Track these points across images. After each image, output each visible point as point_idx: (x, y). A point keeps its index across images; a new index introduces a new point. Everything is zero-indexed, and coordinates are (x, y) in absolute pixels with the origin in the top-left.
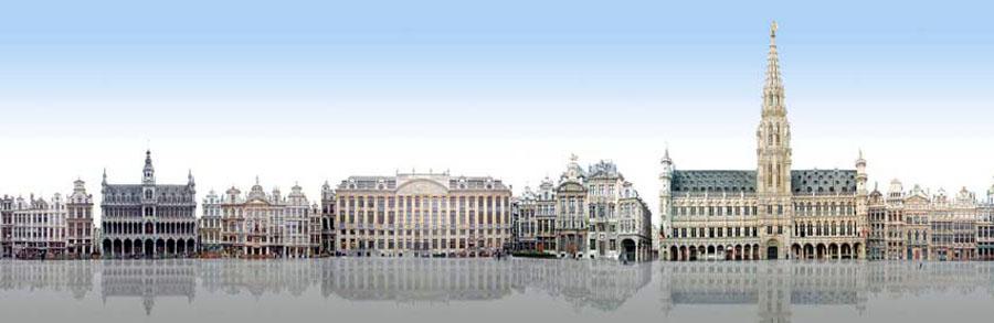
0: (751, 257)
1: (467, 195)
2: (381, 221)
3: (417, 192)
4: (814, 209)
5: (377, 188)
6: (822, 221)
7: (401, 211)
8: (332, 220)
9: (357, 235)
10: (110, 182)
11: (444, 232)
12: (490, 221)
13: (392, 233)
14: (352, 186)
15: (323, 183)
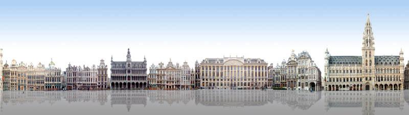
0: (359, 89)
1: (251, 66)
2: (218, 75)
3: (232, 65)
4: (383, 71)
5: (216, 63)
6: (387, 75)
8: (199, 75)
9: (209, 81)
10: (114, 60)
11: (242, 79)
12: (259, 76)
13: (222, 80)
15: (195, 61)
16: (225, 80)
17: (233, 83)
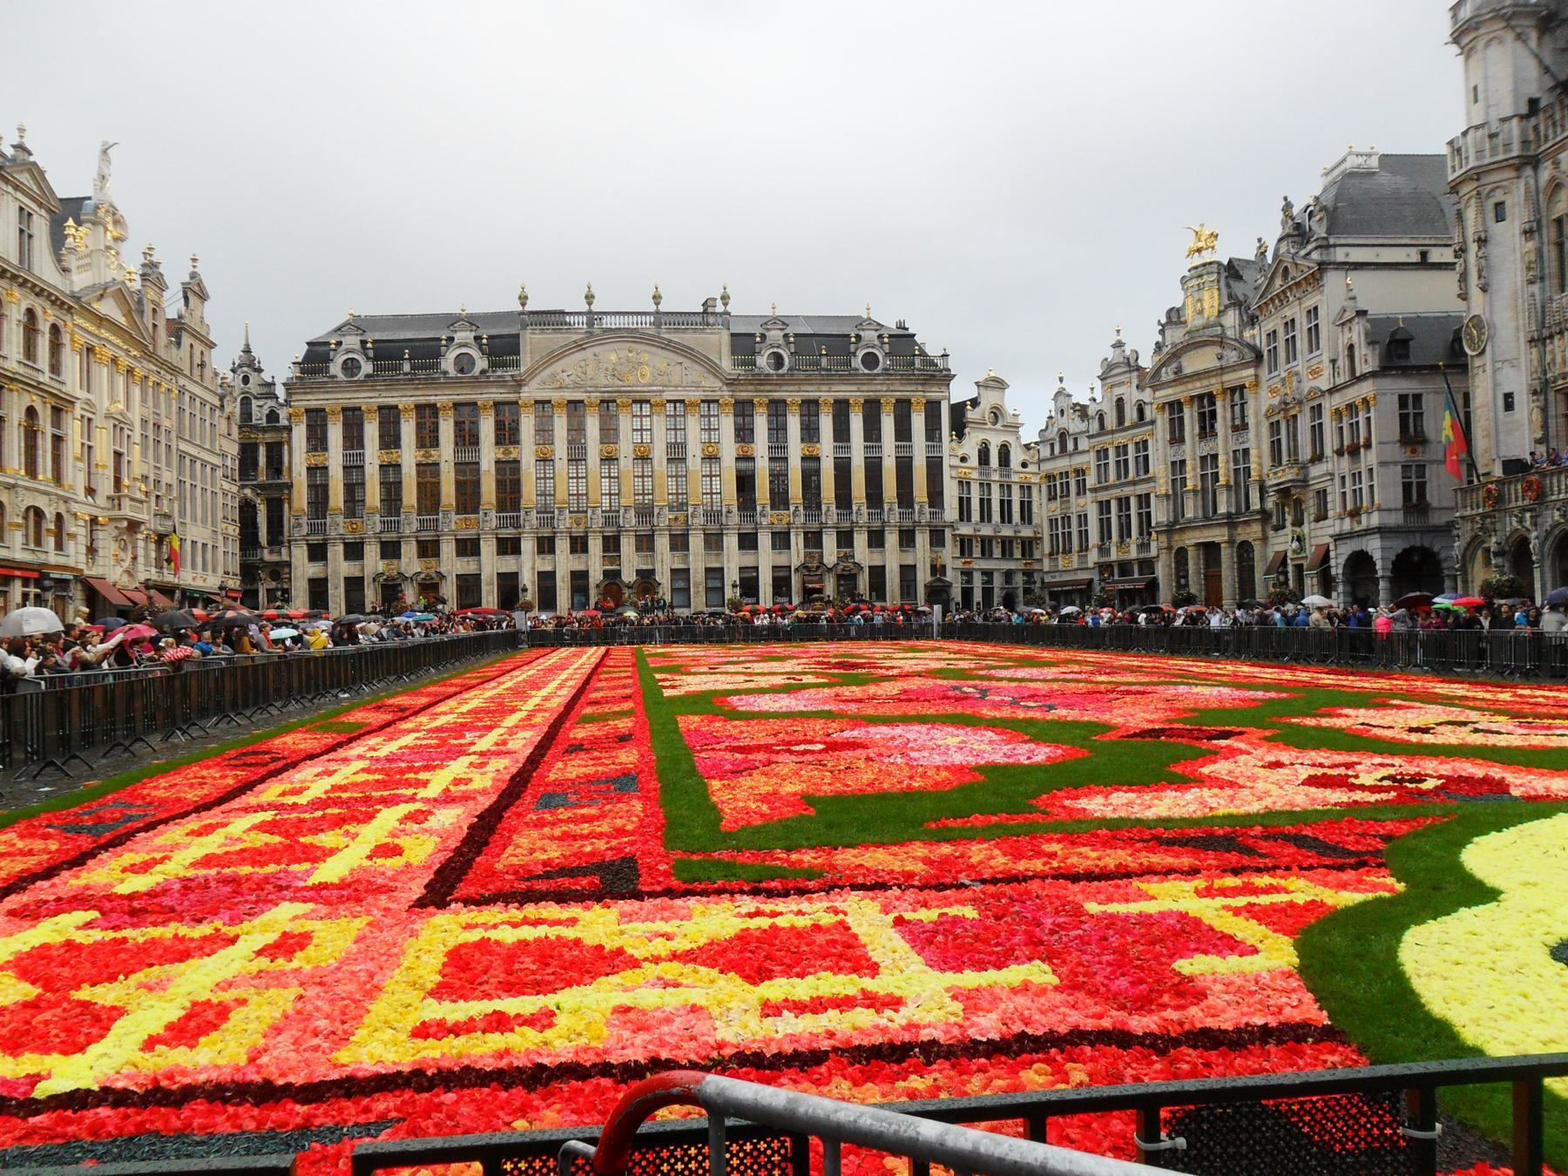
7: (545, 460)
9: (373, 562)
11: (714, 542)
13: (509, 547)
17: (629, 576)
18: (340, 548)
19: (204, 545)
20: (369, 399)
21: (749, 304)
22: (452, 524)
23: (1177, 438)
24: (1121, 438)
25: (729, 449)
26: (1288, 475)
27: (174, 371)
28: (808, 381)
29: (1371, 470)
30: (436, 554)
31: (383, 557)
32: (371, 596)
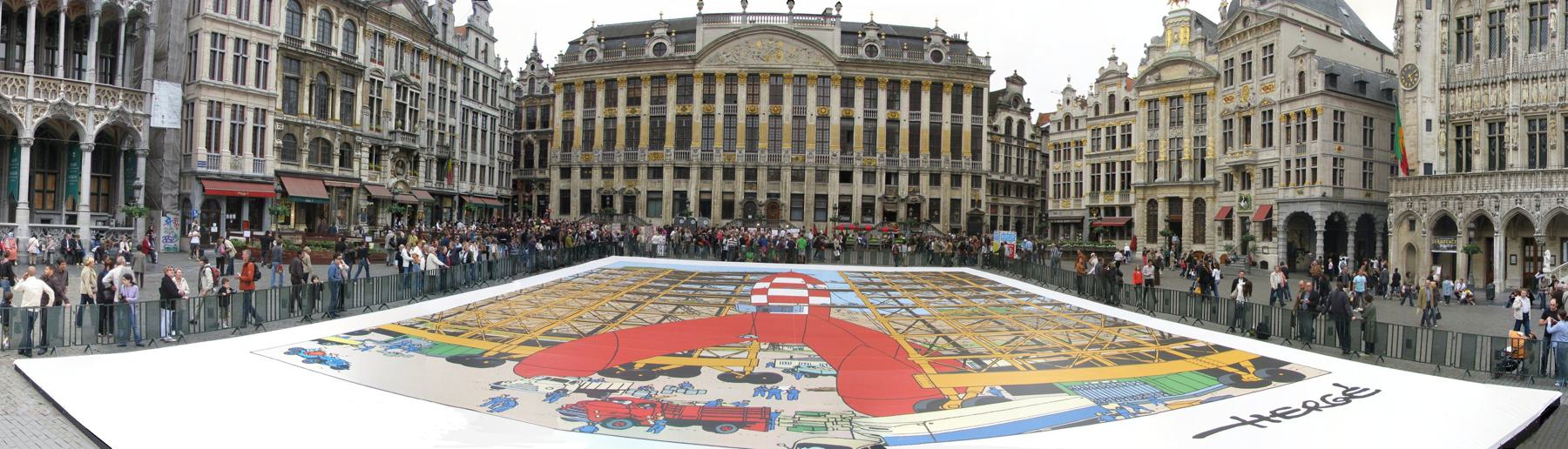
3: (753, 62)
5: (649, 52)
11: (822, 176)
12: (935, 151)
13: (682, 173)
14: (591, 55)
16: (706, 174)
17: (762, 198)
18: (579, 171)
19: (483, 167)
20: (600, 75)
21: (853, 14)
22: (645, 155)
23: (1153, 124)
24: (1111, 122)
25: (836, 111)
26: (1238, 154)
27: (461, 54)
28: (893, 66)
29: (1314, 160)
30: (635, 176)
31: (604, 176)
32: (595, 201)
